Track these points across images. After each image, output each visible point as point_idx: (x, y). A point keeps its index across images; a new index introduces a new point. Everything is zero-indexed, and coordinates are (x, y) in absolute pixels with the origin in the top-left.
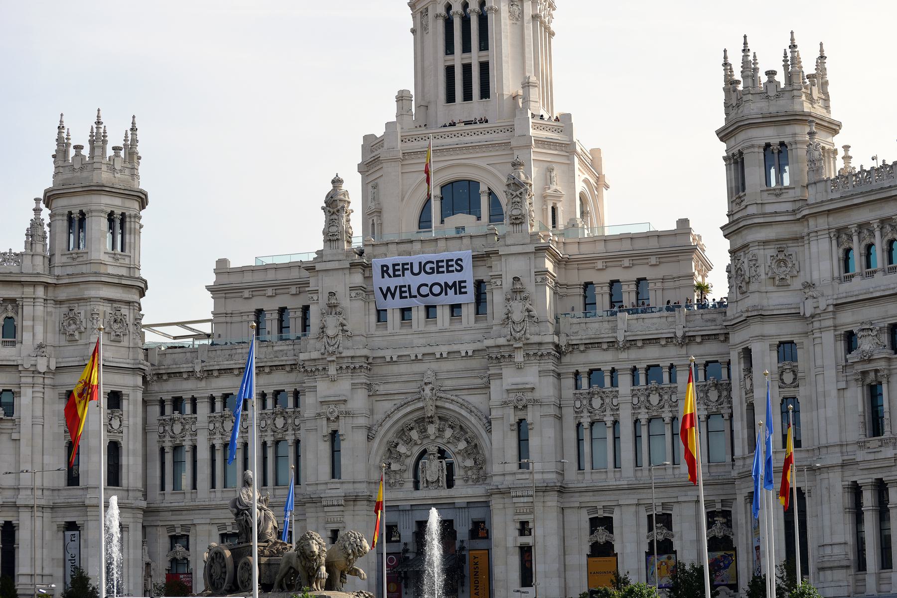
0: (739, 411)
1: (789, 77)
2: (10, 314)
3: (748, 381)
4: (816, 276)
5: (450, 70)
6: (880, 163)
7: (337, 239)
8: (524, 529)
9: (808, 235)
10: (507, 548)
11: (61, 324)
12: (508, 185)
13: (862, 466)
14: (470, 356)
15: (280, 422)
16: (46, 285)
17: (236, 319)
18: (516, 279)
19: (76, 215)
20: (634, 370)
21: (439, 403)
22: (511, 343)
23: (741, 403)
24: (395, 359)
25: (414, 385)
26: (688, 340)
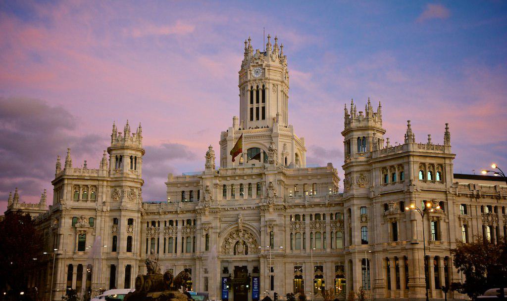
0: (346, 230)
1: (367, 114)
3: (350, 220)
5: (252, 109)
6: (398, 145)
8: (272, 271)
9: (372, 169)
10: (265, 277)
12: (269, 150)
13: (390, 252)
15: (188, 230)
16: (107, 181)
19: (119, 157)
20: (311, 215)
23: (347, 228)
25: (235, 218)
26: (330, 205)
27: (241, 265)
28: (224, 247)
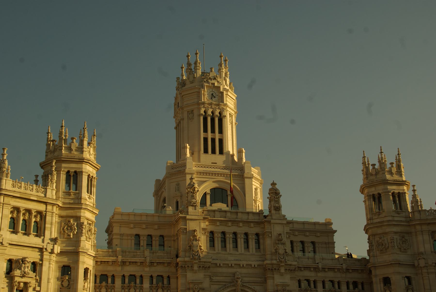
4: (422, 250)
5: (206, 140)
7: (196, 205)
11: (62, 228)
14: (256, 267)
17: (124, 237)
21: (242, 288)
22: (279, 263)
24: (221, 265)
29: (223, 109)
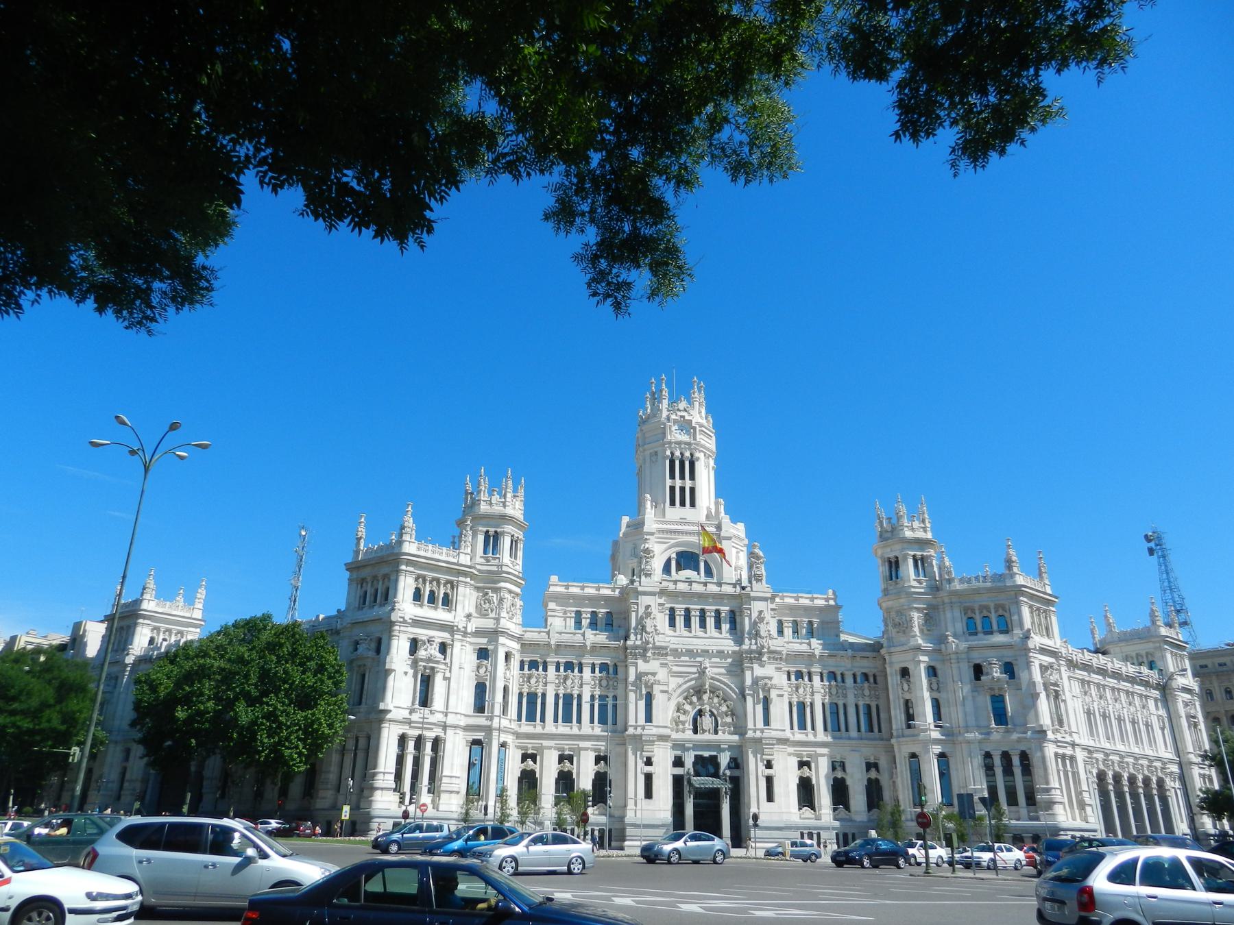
2: (448, 591)
5: (672, 489)
8: (769, 765)
18: (761, 612)
23: (899, 698)
27: (706, 754)
28: (677, 722)
29: (696, 449)
